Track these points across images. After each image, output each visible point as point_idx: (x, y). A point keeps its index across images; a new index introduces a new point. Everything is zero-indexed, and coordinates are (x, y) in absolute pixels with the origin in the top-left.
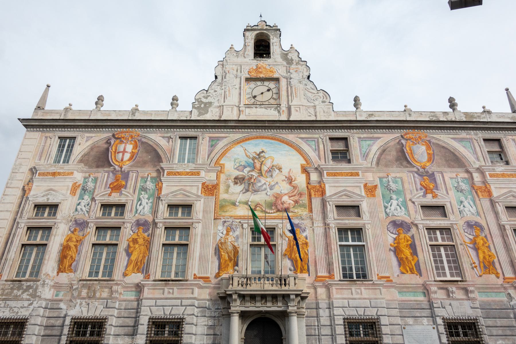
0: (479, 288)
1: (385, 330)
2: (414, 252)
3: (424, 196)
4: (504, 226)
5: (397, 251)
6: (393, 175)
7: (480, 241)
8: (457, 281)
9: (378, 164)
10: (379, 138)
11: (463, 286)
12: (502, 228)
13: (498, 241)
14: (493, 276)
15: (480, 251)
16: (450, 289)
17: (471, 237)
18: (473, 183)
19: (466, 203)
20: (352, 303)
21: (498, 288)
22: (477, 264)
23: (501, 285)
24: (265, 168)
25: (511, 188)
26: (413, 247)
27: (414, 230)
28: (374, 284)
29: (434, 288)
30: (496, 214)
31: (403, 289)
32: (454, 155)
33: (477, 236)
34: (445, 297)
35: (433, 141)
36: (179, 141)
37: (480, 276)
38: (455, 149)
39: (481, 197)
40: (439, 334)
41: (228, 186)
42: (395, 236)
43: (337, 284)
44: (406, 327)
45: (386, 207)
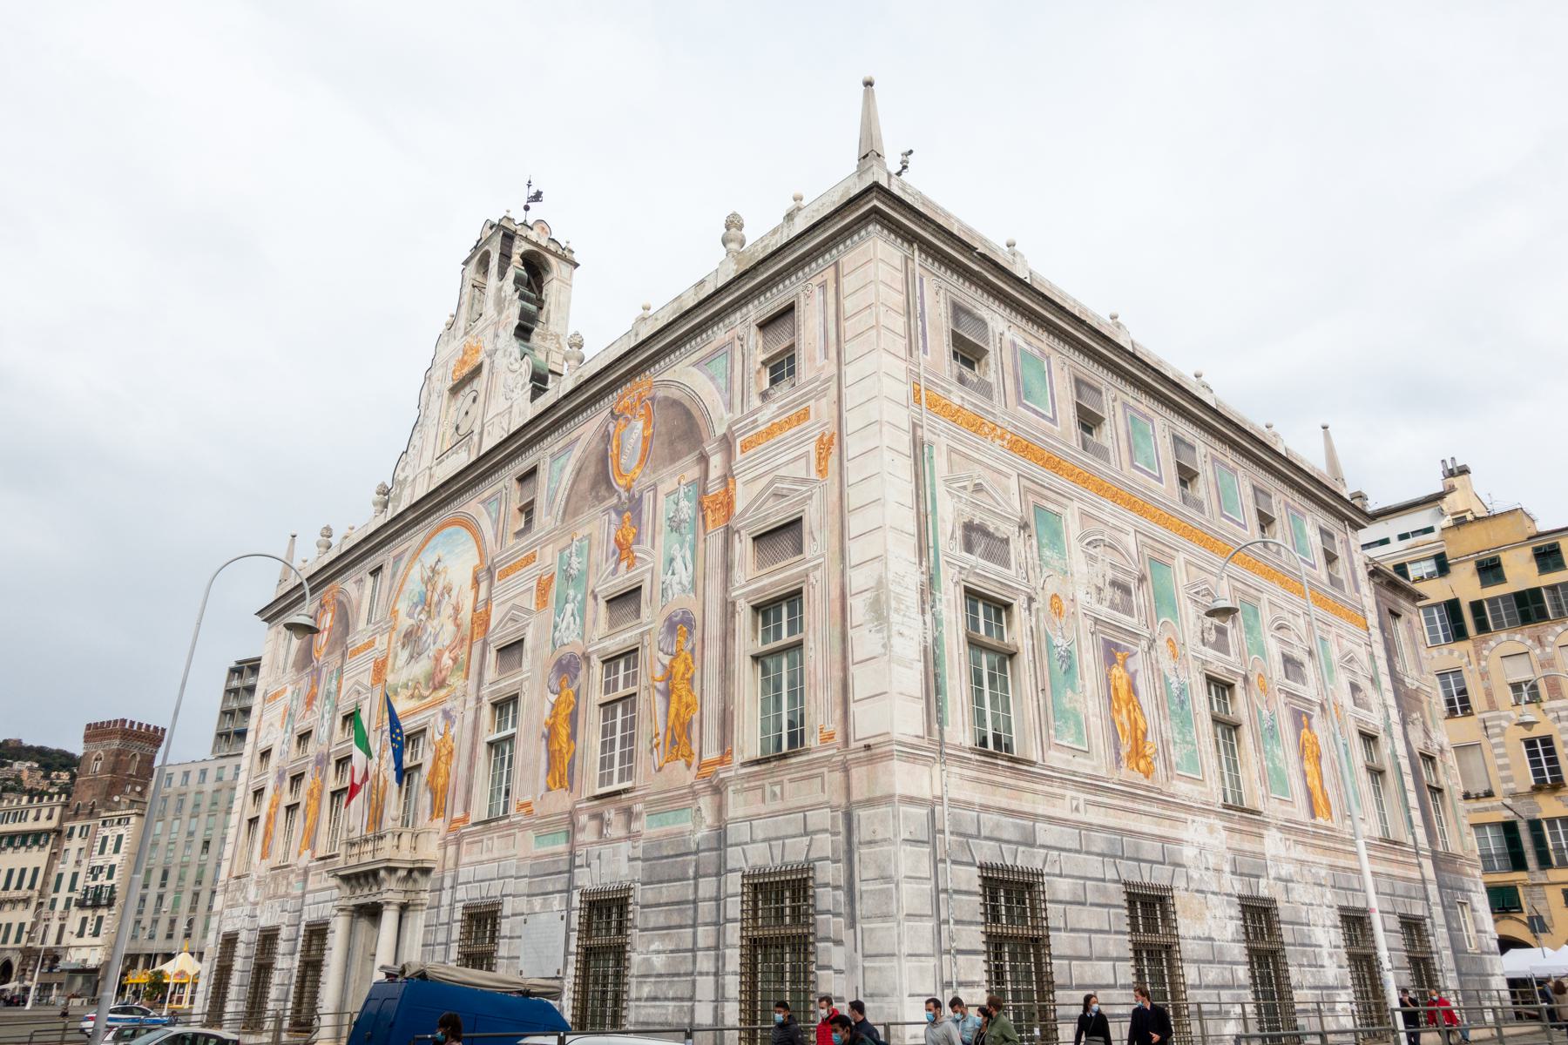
0: (650, 804)
1: (505, 927)
2: (573, 736)
3: (615, 572)
4: (734, 604)
5: (550, 736)
6: (581, 533)
7: (680, 668)
8: (617, 793)
9: (565, 512)
10: (578, 439)
11: (625, 804)
12: (729, 610)
13: (713, 653)
14: (681, 763)
15: (674, 698)
16: (606, 816)
17: (666, 660)
18: (705, 492)
19: (678, 564)
20: (481, 872)
21: (683, 796)
22: (660, 738)
23: (691, 786)
24: (436, 598)
25: (778, 467)
26: (573, 718)
27: (582, 673)
28: (511, 825)
29: (583, 818)
30: (728, 567)
31: (544, 827)
32: (688, 414)
33: (675, 656)
34: (595, 839)
35: (661, 393)
36: (369, 580)
37: (660, 769)
38: (695, 397)
39: (710, 529)
40: (568, 930)
41: (396, 656)
42: (553, 698)
43: (470, 833)
44: (530, 919)
45: (555, 627)
